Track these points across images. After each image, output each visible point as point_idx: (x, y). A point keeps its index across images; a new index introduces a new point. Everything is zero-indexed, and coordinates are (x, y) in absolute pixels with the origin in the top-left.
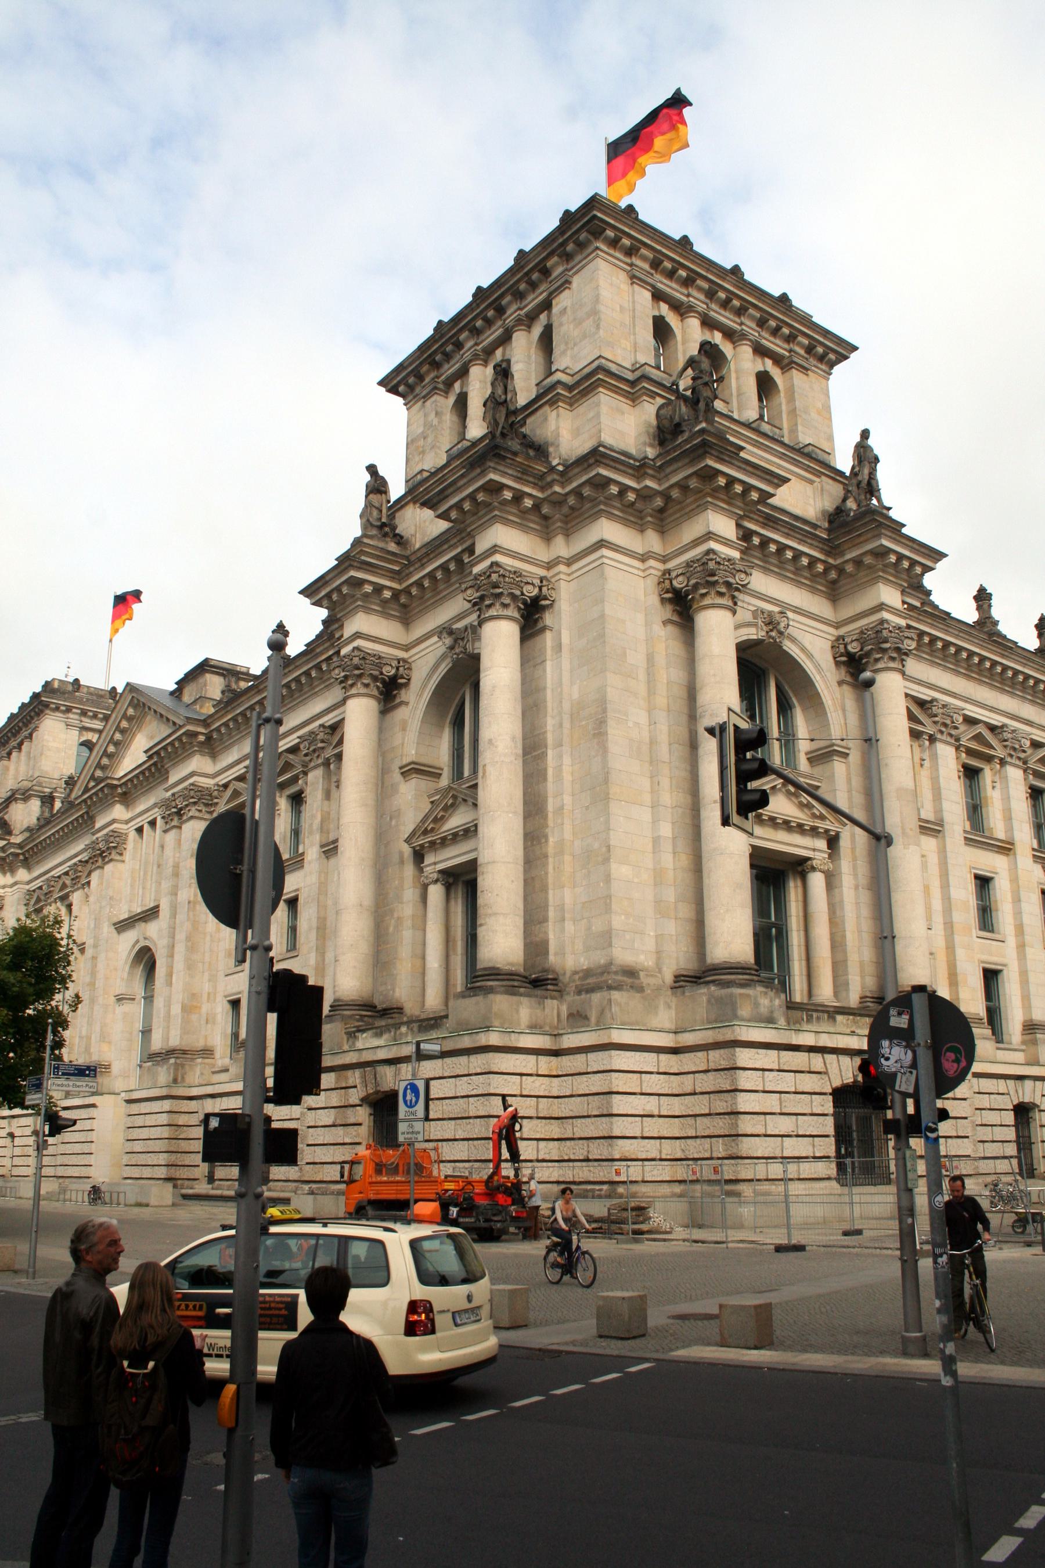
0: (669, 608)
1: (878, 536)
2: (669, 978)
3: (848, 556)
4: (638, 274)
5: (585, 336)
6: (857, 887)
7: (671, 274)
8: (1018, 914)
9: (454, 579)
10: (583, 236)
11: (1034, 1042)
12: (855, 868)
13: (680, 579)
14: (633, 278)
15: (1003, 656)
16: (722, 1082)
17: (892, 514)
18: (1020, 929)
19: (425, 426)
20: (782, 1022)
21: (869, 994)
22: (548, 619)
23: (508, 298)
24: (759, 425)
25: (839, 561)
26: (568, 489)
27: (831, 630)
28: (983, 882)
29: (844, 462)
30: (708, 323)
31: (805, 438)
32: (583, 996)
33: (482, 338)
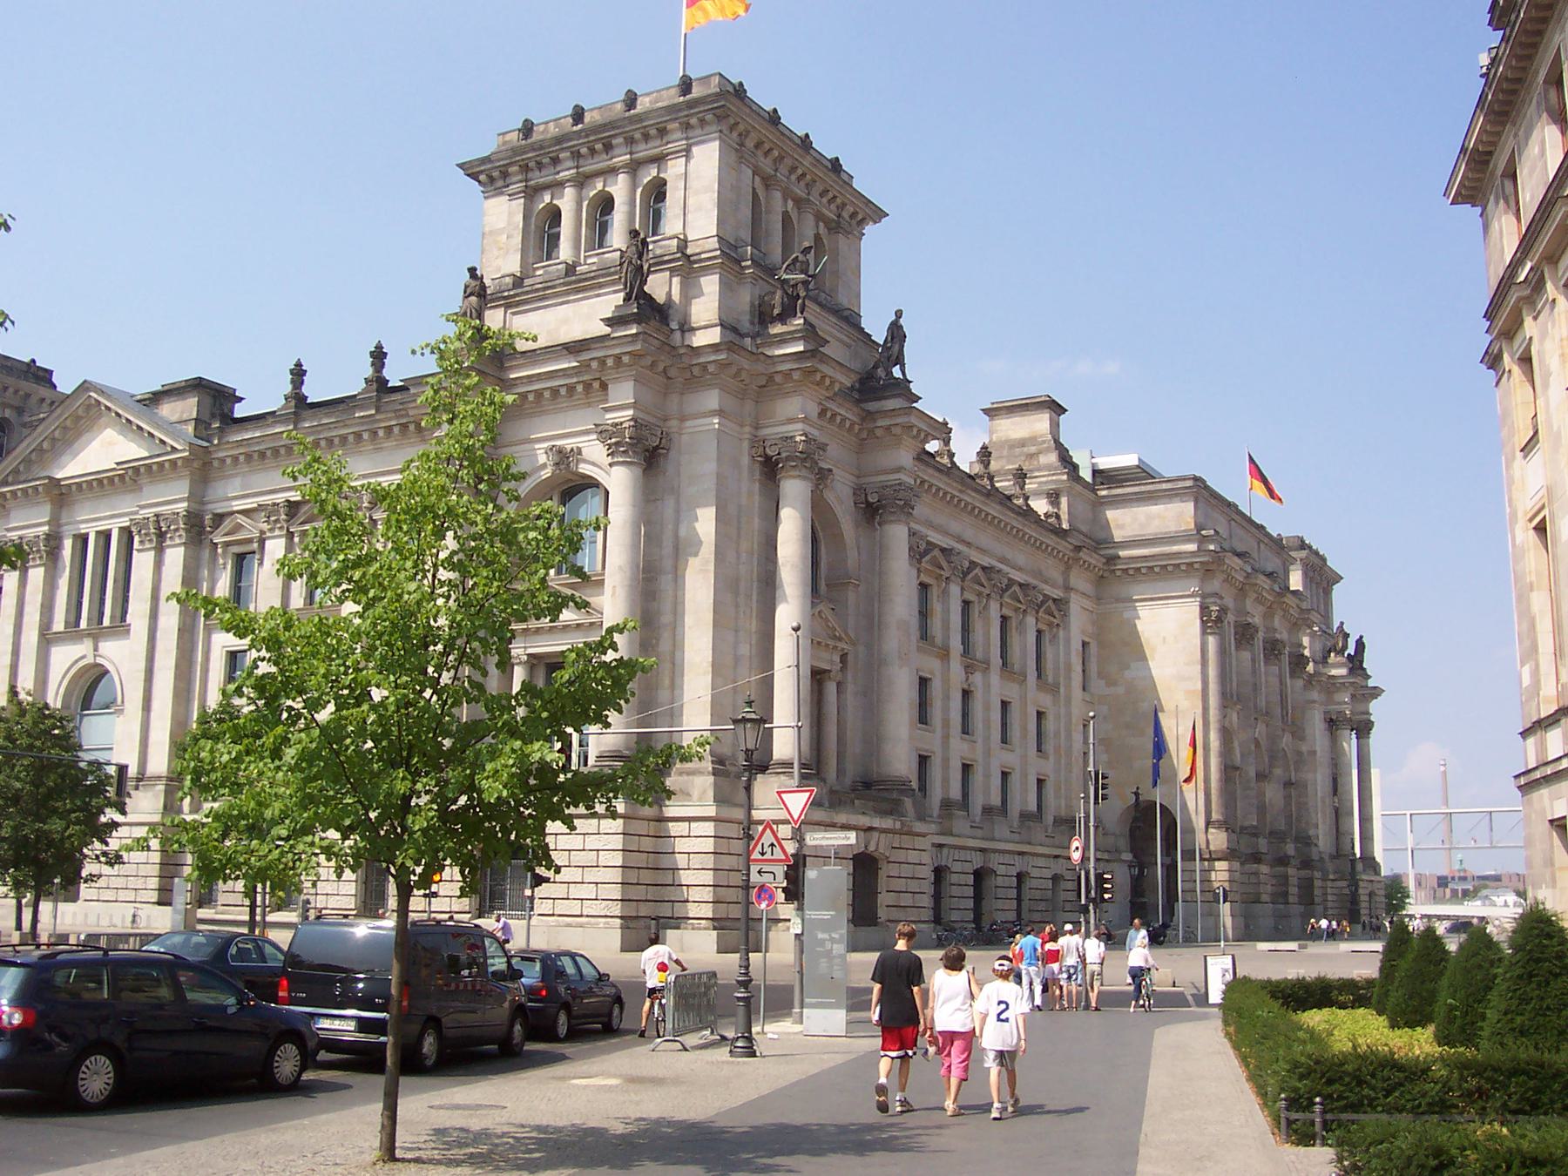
1: (910, 414)
4: (746, 156)
8: (946, 710)
9: (560, 400)
10: (709, 117)
11: (950, 816)
13: (773, 448)
15: (961, 491)
18: (946, 723)
19: (509, 223)
20: (827, 804)
21: (858, 779)
23: (620, 140)
24: (818, 295)
25: (871, 425)
28: (924, 682)
29: (880, 336)
31: (843, 300)
32: (685, 777)
33: (582, 162)
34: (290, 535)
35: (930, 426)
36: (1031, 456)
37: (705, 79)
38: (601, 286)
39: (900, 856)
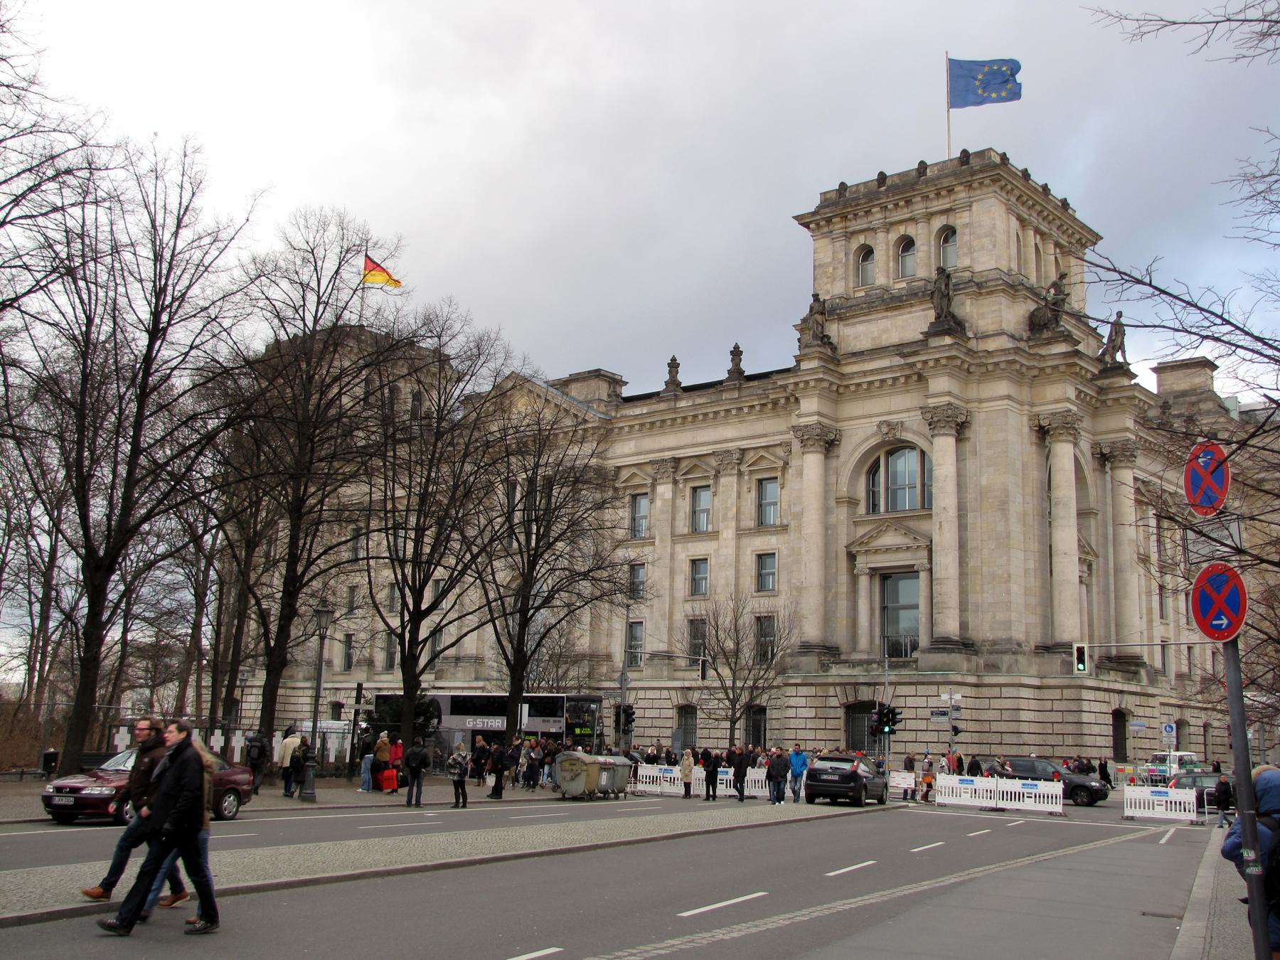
0: (1034, 434)
2: (1033, 648)
3: (1111, 396)
5: (983, 248)
6: (1098, 593)
7: (1023, 204)
10: (987, 182)
12: (1098, 581)
14: (1009, 210)
16: (1073, 706)
17: (1131, 367)
22: (968, 433)
23: (919, 199)
25: (1104, 398)
26: (991, 361)
27: (1090, 436)
30: (1037, 231)
34: (675, 482)
35: (1147, 396)
36: (1193, 404)
37: (981, 154)
38: (912, 305)
39: (1140, 711)
